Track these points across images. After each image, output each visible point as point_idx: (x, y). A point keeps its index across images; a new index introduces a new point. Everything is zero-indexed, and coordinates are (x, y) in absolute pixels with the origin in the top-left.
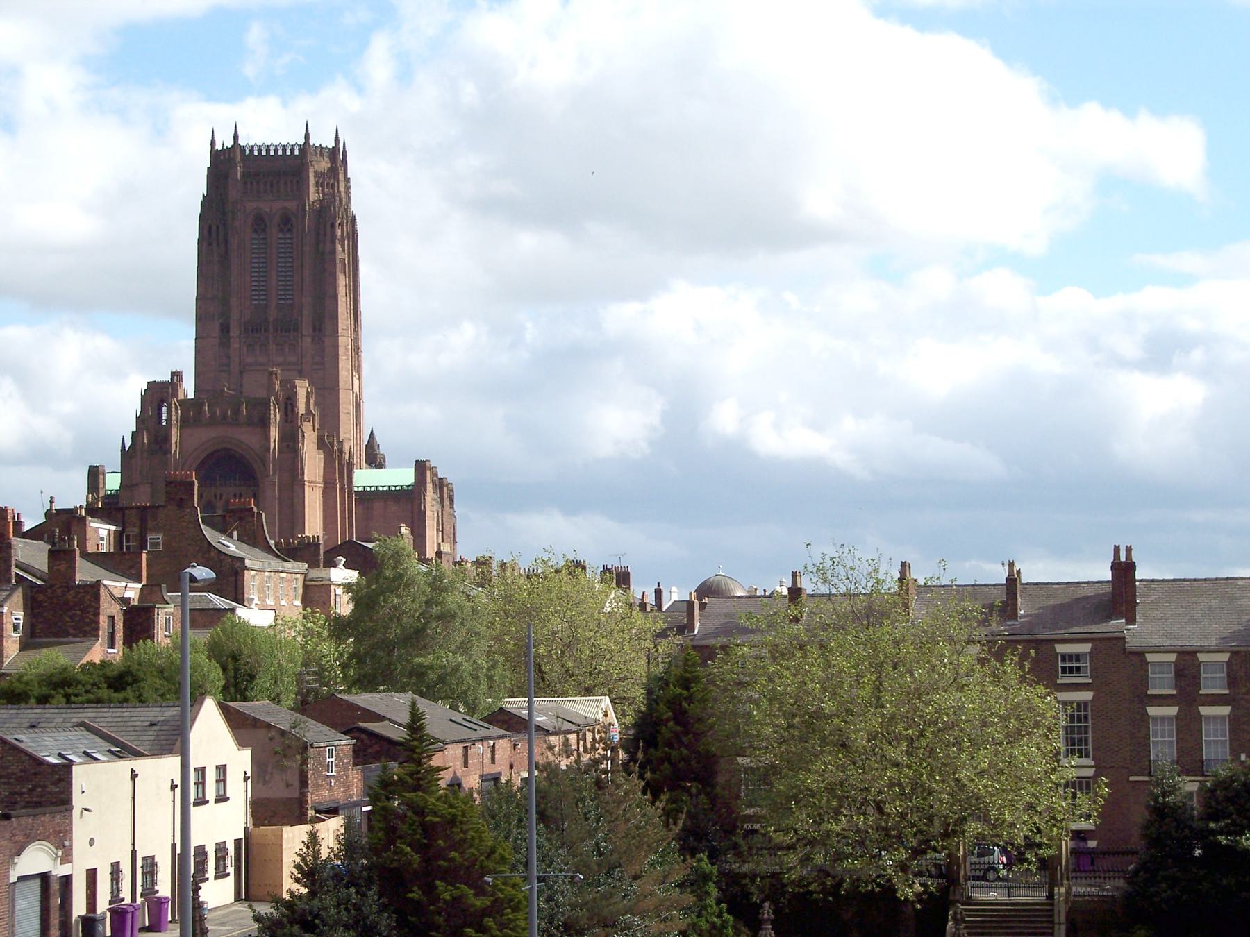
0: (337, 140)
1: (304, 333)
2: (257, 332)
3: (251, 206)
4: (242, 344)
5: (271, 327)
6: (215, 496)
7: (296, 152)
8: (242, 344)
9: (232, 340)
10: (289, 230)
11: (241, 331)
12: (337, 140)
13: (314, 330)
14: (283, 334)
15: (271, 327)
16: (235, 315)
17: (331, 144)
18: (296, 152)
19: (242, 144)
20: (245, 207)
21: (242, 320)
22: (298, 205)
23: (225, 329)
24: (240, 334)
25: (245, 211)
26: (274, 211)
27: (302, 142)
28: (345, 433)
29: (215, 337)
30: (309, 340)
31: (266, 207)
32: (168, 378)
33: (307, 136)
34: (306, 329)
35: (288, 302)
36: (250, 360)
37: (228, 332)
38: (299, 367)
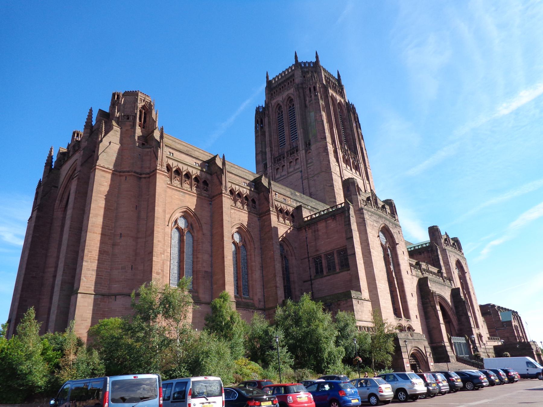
0: (317, 57)
1: (301, 149)
2: (280, 160)
4: (273, 169)
5: (286, 155)
11: (272, 163)
12: (317, 57)
15: (286, 155)
16: (268, 155)
17: (314, 60)
20: (271, 104)
21: (273, 157)
23: (266, 165)
24: (272, 165)
25: (272, 106)
26: (284, 98)
28: (330, 198)
29: (261, 171)
30: (304, 151)
34: (301, 146)
38: (300, 170)
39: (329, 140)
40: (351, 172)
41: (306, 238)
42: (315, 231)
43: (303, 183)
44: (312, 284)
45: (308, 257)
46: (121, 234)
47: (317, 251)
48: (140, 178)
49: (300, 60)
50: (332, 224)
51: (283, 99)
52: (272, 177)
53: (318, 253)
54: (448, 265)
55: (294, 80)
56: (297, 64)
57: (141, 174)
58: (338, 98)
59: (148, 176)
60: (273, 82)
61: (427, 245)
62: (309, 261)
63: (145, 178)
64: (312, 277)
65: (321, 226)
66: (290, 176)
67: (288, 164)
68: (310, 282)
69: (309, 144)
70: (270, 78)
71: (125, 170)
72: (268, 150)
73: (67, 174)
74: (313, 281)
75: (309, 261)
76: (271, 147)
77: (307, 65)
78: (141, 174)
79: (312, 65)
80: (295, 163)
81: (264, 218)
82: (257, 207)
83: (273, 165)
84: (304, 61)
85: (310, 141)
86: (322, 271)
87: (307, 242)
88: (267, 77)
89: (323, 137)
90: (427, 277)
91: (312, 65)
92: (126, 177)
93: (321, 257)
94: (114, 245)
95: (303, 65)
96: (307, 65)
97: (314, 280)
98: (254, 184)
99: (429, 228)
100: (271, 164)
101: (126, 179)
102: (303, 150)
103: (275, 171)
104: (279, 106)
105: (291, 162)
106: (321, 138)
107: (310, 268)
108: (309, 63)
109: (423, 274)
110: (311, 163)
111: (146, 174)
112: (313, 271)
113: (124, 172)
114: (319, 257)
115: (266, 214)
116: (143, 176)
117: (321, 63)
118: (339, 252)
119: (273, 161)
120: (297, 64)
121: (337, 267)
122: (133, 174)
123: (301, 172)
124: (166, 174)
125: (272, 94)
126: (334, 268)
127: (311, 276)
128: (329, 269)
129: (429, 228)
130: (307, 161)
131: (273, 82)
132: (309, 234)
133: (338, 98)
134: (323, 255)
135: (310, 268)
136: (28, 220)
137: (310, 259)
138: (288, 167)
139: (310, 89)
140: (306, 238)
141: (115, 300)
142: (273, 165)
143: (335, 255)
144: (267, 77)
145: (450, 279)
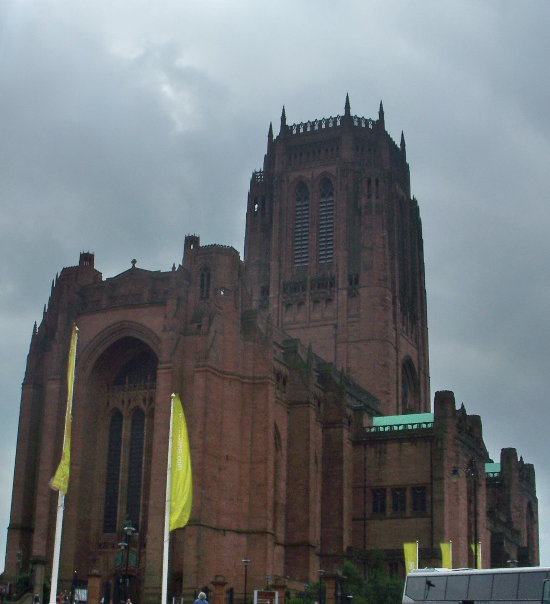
0: (381, 113)
1: (340, 286)
3: (293, 176)
6: (123, 402)
7: (338, 124)
8: (280, 304)
9: (271, 301)
10: (331, 194)
12: (381, 113)
13: (351, 283)
14: (321, 290)
16: (274, 276)
17: (376, 118)
18: (338, 124)
19: (289, 125)
21: (282, 281)
22: (337, 168)
24: (279, 294)
27: (342, 113)
30: (345, 293)
31: (307, 175)
32: (75, 262)
33: (347, 107)
34: (342, 282)
35: (328, 261)
36: (287, 319)
37: (268, 294)
39: (389, 284)
40: (406, 337)
41: (365, 459)
42: (380, 452)
43: (336, 347)
44: (365, 525)
45: (365, 487)
46: (227, 456)
47: (380, 480)
48: (243, 383)
49: (352, 114)
50: (409, 449)
51: (312, 177)
52: (278, 317)
53: (382, 484)
54: (518, 511)
55: (338, 148)
56: (347, 118)
57: (243, 378)
58: (401, 192)
59: (251, 381)
60: (294, 132)
61: (496, 475)
62: (365, 492)
63: (248, 383)
64: (368, 516)
65: (392, 448)
66: (314, 326)
67: (312, 303)
68: (362, 522)
69: (357, 281)
70: (289, 123)
71: (228, 370)
72: (274, 264)
73: (98, 334)
74: (368, 521)
75: (365, 492)
76: (280, 261)
77: (363, 125)
78: (243, 378)
79: (370, 126)
80: (324, 306)
81: (332, 430)
82: (322, 410)
83: (281, 296)
84: (360, 116)
85: (358, 276)
86: (383, 509)
87: (365, 464)
88: (283, 119)
89: (381, 278)
90: (502, 534)
91: (370, 126)
92: (230, 381)
93: (385, 490)
94: (220, 469)
95: (356, 124)
96: (363, 125)
97: (369, 519)
98: (318, 374)
99: (503, 450)
100: (277, 293)
101: (230, 385)
102: (343, 289)
103: (284, 309)
104: (301, 185)
105: (316, 302)
106: (380, 280)
107: (365, 503)
108: (367, 122)
109: (495, 526)
110: (353, 317)
111: (249, 378)
112: (369, 507)
113: (227, 374)
114: (383, 490)
115: (336, 425)
116: (246, 381)
117: (388, 128)
118: (414, 489)
119: (282, 289)
120: (347, 118)
121: (409, 511)
122: (238, 378)
123: (336, 327)
124: (274, 383)
125: (290, 157)
126: (403, 509)
127: (365, 514)
128: (395, 508)
129: (503, 450)
130: (348, 310)
131: (294, 132)
132: (371, 453)
133: (401, 192)
134: (388, 489)
135: (365, 503)
136: (22, 384)
137: (368, 490)
138: (312, 309)
139: (369, 183)
140: (365, 459)
141: (225, 535)
142: (281, 296)
143: (408, 494)
144: (283, 119)
145: (517, 533)
